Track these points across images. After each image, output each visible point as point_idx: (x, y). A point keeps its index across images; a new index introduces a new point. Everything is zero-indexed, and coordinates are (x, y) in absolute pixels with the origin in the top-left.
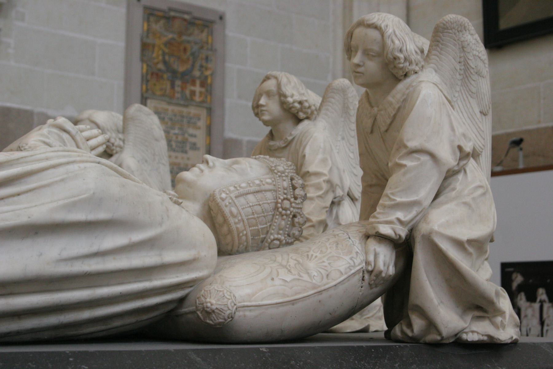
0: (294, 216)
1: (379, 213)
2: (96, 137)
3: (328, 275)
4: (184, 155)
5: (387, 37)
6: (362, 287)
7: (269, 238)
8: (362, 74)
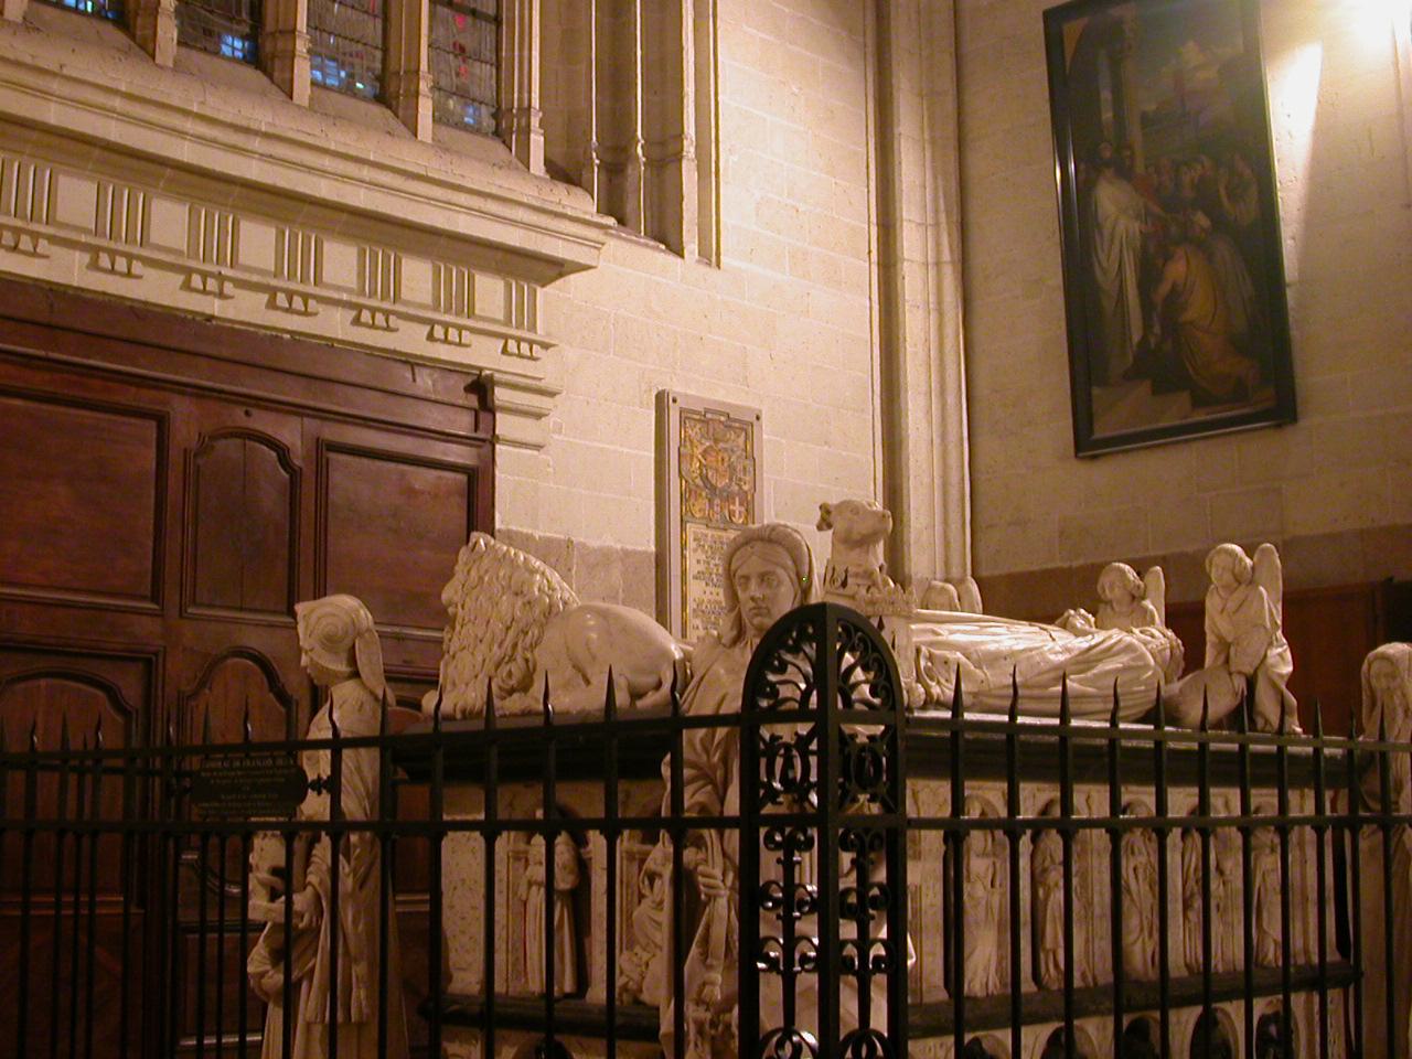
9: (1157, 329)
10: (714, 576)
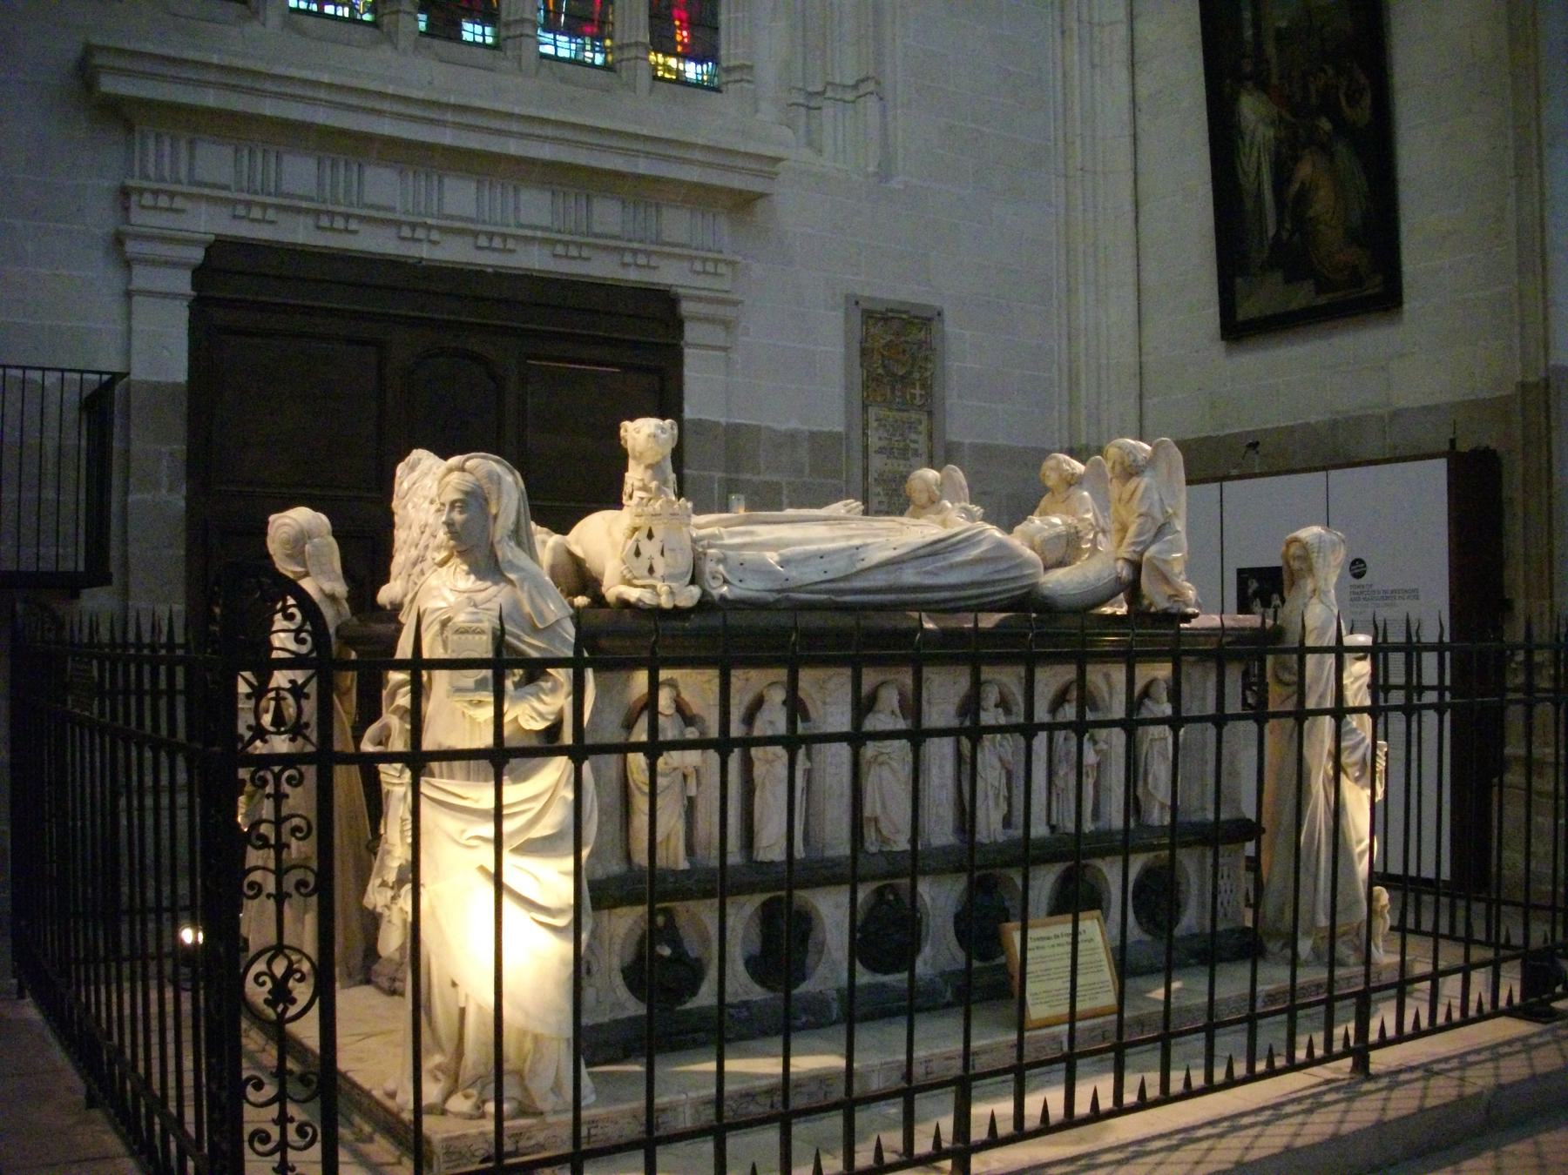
9: (1288, 226)
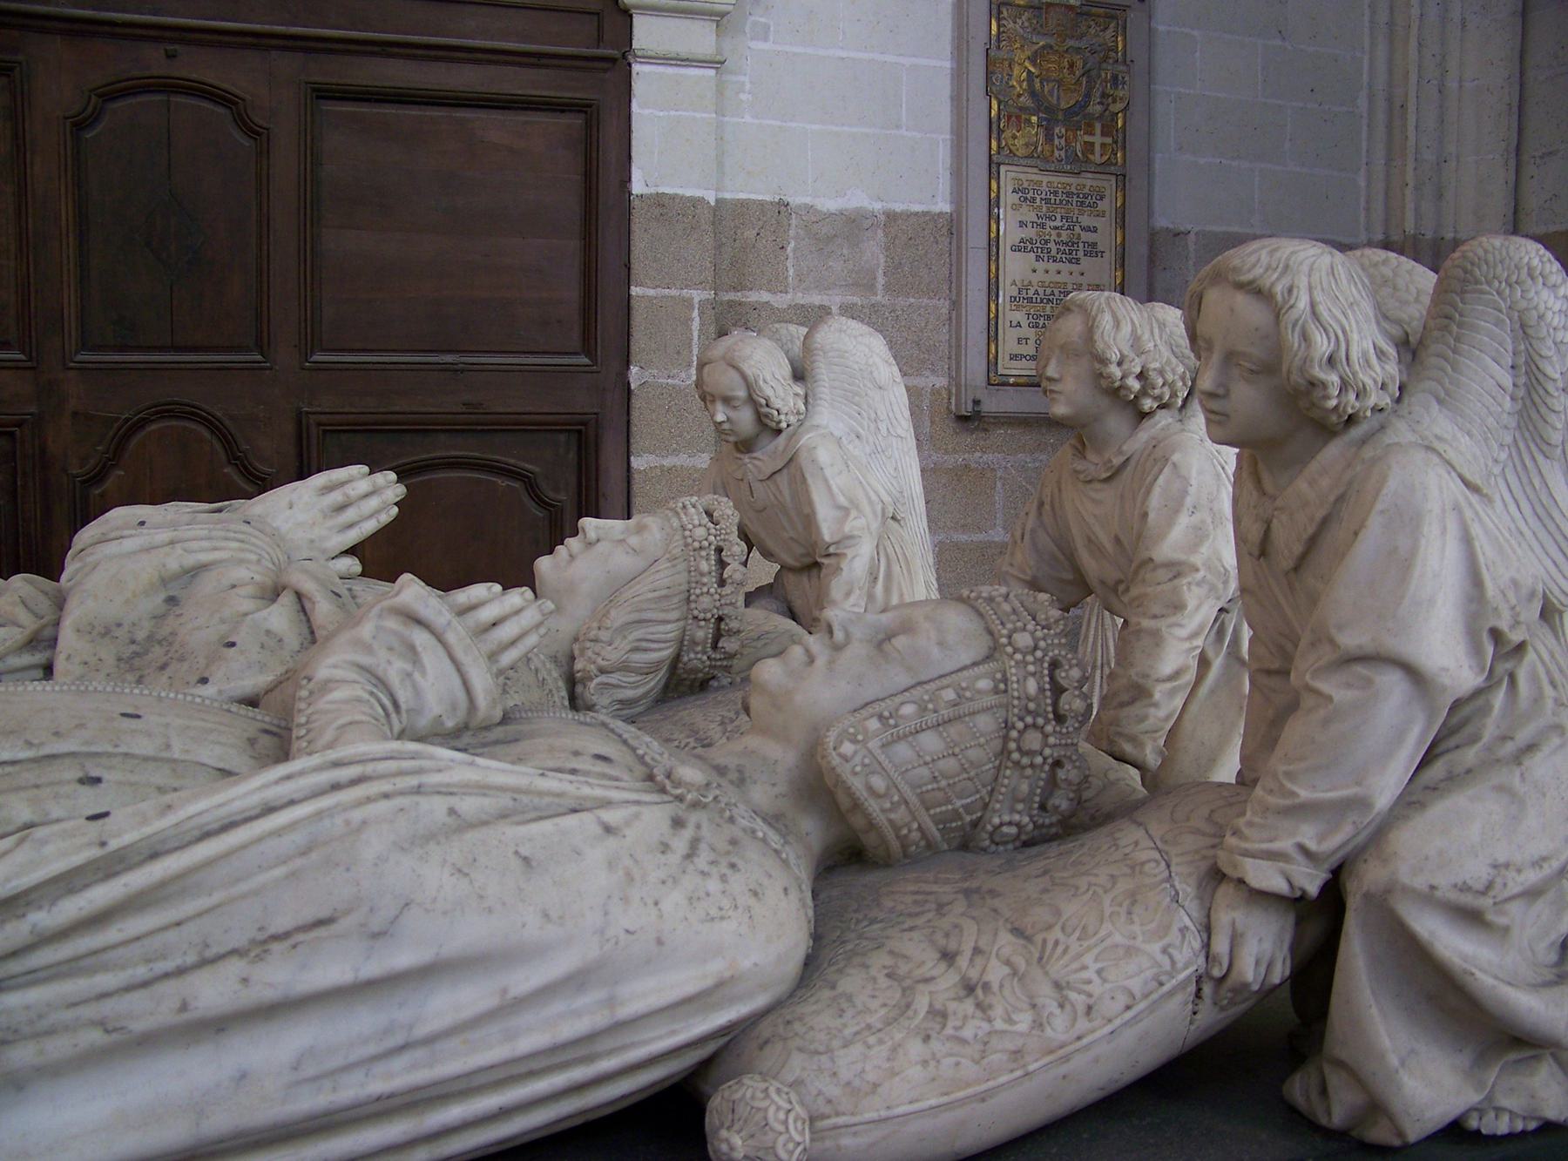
0: (1057, 764)
1: (1250, 824)
2: (518, 612)
3: (1090, 1008)
4: (1073, 267)
5: (1290, 326)
6: (1195, 1013)
7: (990, 823)
8: (1222, 418)
10: (1052, 245)
